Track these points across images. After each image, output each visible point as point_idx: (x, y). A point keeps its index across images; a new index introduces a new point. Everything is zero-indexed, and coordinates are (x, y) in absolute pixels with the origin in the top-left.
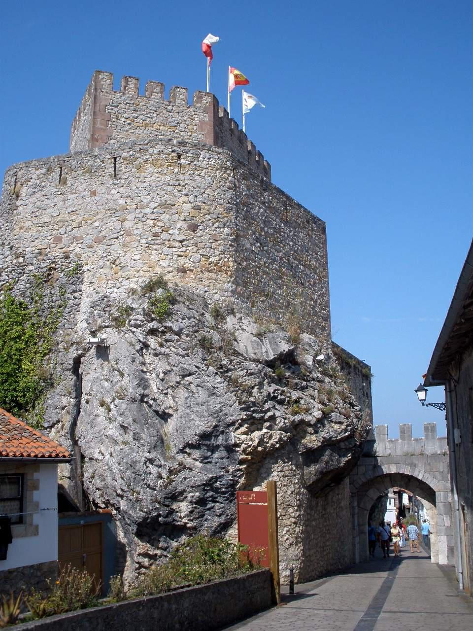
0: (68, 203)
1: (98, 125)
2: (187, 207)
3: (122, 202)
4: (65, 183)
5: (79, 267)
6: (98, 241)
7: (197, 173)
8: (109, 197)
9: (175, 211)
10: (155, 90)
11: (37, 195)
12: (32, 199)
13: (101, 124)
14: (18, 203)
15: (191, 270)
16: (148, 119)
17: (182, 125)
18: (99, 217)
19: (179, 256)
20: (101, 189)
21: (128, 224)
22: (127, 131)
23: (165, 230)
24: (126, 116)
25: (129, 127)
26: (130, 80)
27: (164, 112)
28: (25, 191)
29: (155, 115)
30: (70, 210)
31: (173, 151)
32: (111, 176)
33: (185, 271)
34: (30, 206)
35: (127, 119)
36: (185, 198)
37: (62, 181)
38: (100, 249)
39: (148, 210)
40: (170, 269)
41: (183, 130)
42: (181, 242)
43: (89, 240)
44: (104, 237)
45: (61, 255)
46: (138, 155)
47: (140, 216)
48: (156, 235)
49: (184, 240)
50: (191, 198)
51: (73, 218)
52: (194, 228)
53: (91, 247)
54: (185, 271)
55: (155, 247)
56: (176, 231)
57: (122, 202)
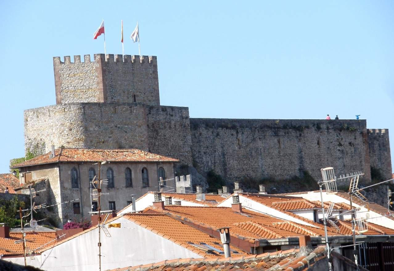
0: (40, 124)
1: (57, 80)
2: (68, 124)
3: (52, 124)
4: (38, 117)
5: (44, 143)
6: (48, 135)
7: (70, 113)
8: (49, 122)
9: (65, 126)
10: (76, 59)
11: (32, 120)
12: (31, 122)
13: (58, 79)
14: (28, 123)
15: (71, 142)
16: (75, 72)
17: (89, 71)
18: (47, 128)
19: (67, 139)
20: (47, 120)
21: (54, 131)
22: (68, 79)
23: (63, 132)
24: (66, 73)
25: (68, 78)
26: (66, 58)
27: (81, 67)
28: (29, 119)
29: (77, 70)
30: (40, 126)
31: (63, 108)
32: (49, 116)
33: (69, 143)
34: (30, 124)
35: (67, 74)
36: (67, 122)
37: (38, 117)
38: (48, 137)
39: (58, 127)
40: (65, 143)
41: (89, 73)
42: (67, 134)
43: (46, 135)
44: (49, 134)
45: (40, 139)
46: (54, 110)
47: (56, 128)
48: (61, 133)
49: (68, 134)
50: (69, 121)
51: (41, 128)
52: (71, 130)
53: (46, 137)
54: (69, 143)
55: (60, 137)
56: (66, 132)
57: (52, 124)
